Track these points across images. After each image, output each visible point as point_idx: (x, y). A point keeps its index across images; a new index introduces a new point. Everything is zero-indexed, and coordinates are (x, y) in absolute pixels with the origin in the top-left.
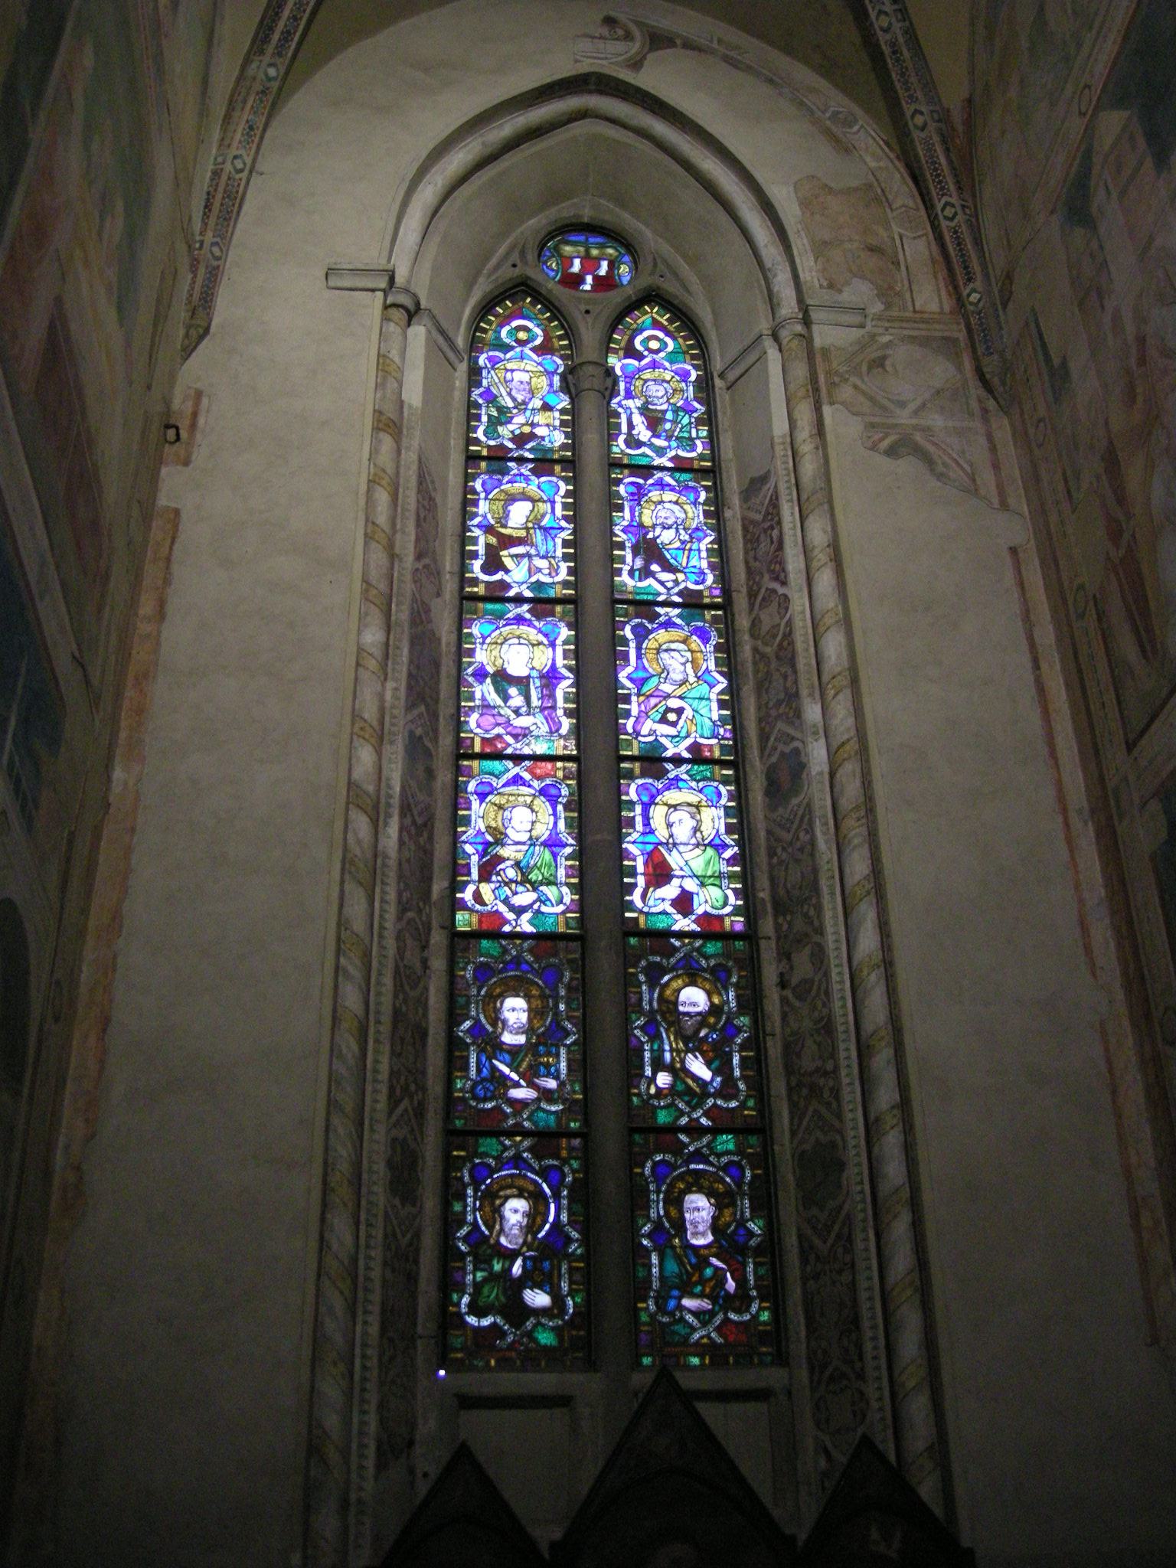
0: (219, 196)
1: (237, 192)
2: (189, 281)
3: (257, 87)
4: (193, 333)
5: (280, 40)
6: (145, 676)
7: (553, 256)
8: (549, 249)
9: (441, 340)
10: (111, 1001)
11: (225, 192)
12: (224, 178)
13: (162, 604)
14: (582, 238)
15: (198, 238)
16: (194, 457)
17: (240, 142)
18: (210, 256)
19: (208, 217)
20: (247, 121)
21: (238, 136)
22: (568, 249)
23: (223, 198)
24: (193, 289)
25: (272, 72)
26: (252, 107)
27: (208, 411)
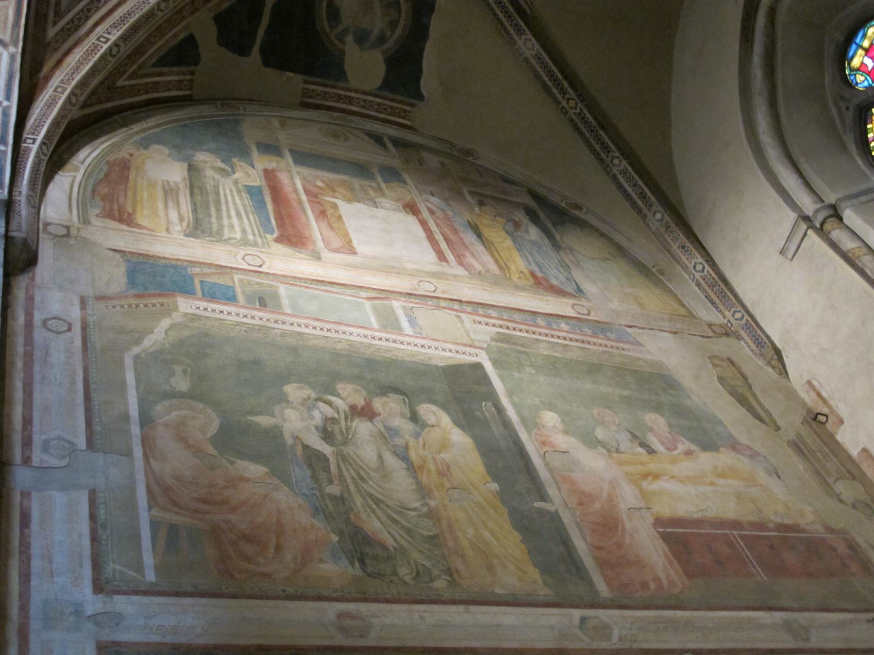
0: (709, 291)
1: (714, 279)
2: (745, 345)
3: (662, 230)
4: (775, 363)
5: (643, 202)
7: (855, 75)
8: (850, 75)
9: (863, 199)
11: (709, 286)
12: (702, 282)
14: (854, 47)
15: (726, 322)
16: (841, 415)
17: (687, 259)
18: (738, 322)
19: (718, 307)
20: (678, 247)
21: (684, 258)
22: (856, 63)
23: (712, 290)
24: (749, 346)
25: (658, 216)
26: (672, 240)
27: (821, 387)
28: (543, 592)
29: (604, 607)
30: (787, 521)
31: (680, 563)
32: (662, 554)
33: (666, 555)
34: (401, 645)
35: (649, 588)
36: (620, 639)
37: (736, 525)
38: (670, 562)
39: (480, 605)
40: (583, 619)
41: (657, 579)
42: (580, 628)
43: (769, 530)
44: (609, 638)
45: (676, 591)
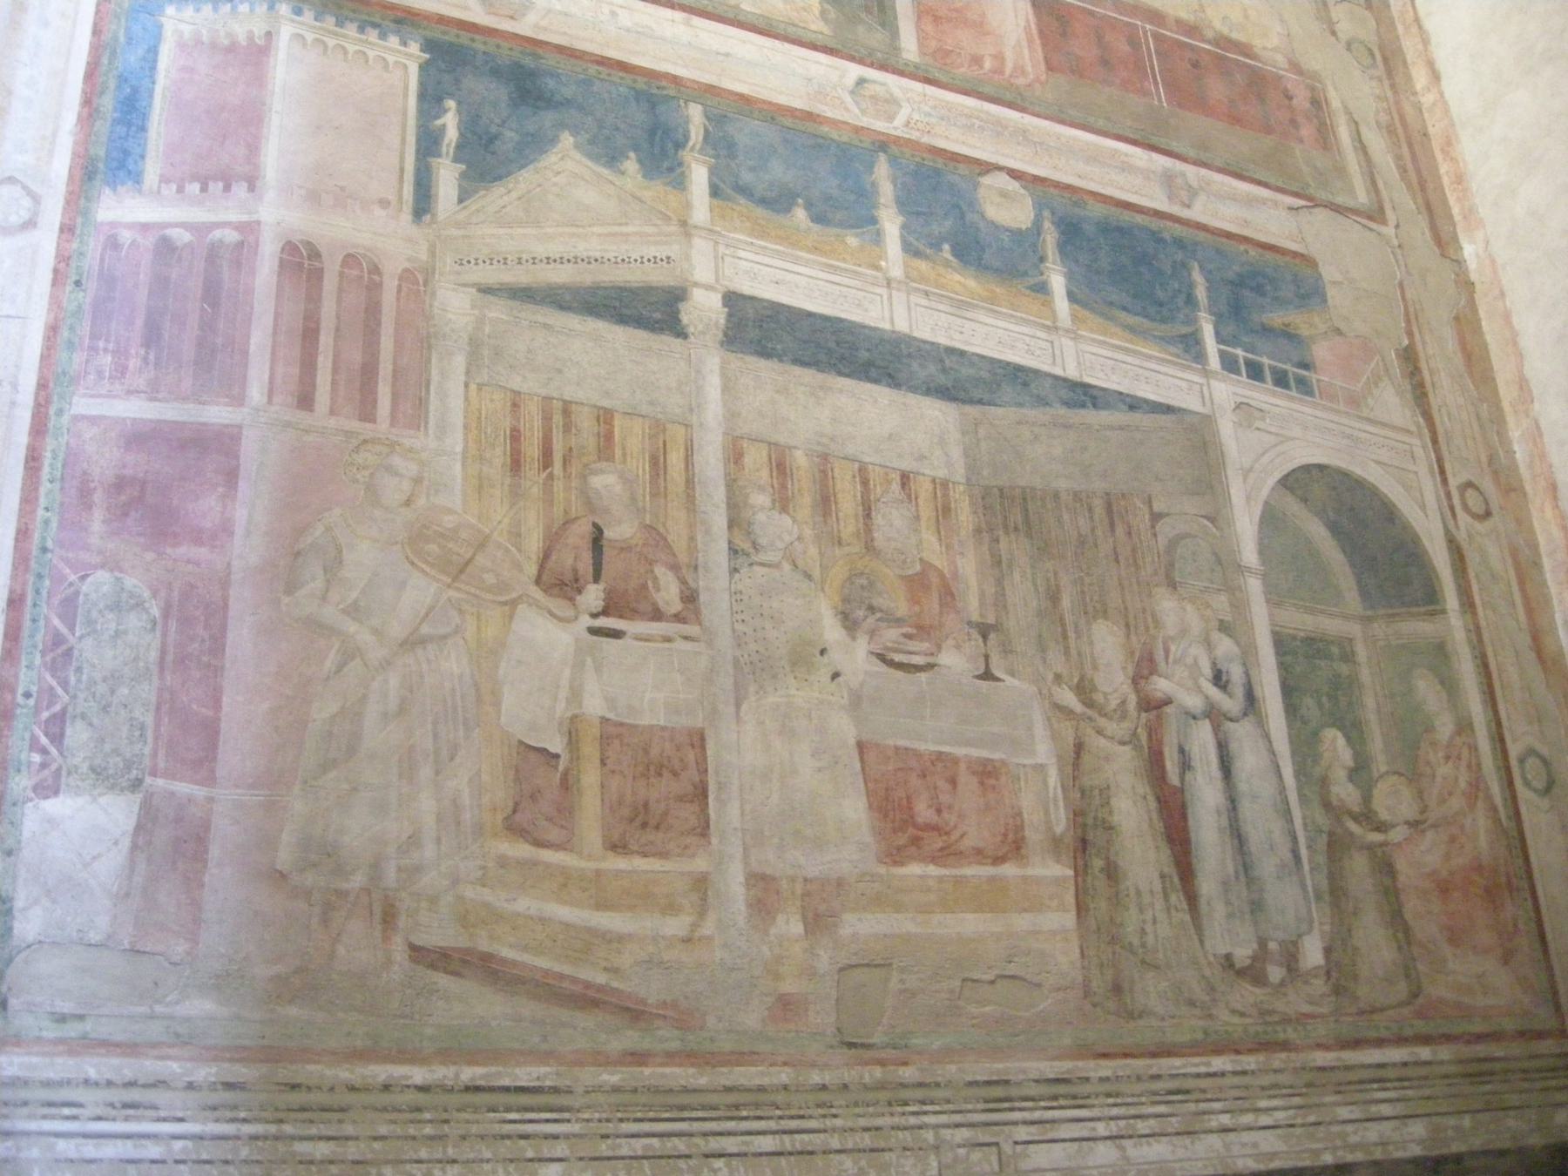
6: (1449, 142)
10: (1551, 466)
13: (1431, 65)
28: (818, 27)
29: (902, 73)
30: (1235, 35)
31: (1044, 45)
32: (1022, 24)
33: (1027, 29)
35: (981, 67)
36: (907, 124)
37: (1156, 17)
38: (1030, 41)
39: (719, 21)
40: (861, 82)
41: (999, 58)
42: (852, 92)
43: (1203, 41)
44: (891, 118)
45: (1021, 81)
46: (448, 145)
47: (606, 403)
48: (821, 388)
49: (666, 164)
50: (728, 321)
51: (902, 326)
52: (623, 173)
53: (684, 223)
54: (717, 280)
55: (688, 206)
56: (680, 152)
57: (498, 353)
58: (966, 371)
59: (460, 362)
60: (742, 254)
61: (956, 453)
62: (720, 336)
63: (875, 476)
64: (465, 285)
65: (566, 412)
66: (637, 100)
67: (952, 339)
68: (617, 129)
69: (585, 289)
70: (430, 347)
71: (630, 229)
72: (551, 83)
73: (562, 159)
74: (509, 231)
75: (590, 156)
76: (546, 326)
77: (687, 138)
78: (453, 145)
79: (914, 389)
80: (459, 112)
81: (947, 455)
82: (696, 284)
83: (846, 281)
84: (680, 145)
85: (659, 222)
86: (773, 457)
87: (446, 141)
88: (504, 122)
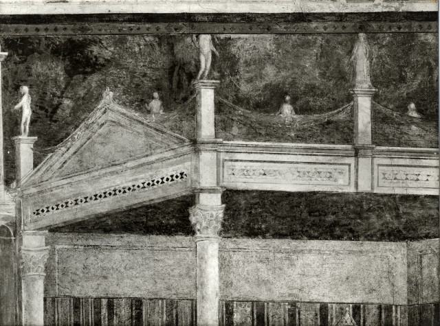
34: (107, 12)
46: (26, 122)
47: (137, 294)
48: (294, 252)
49: (182, 95)
50: (225, 214)
51: (364, 187)
52: (149, 112)
53: (194, 142)
54: (218, 183)
55: (197, 127)
56: (193, 82)
57: (64, 272)
58: (417, 213)
59: (40, 286)
60: (238, 156)
61: (401, 284)
62: (219, 227)
63: (333, 312)
64: (41, 229)
65: (110, 306)
66: (160, 45)
67: (408, 188)
68: (145, 75)
69: (121, 213)
70: (20, 279)
71: (153, 158)
72: (95, 49)
73: (105, 112)
74: (69, 180)
75: (124, 104)
76: (96, 247)
77: (198, 67)
78: (28, 122)
79: (370, 238)
80: (30, 93)
81: (393, 285)
82: (202, 190)
83: (321, 159)
84: (192, 76)
85: (176, 146)
86: (255, 311)
87: (23, 120)
88: (63, 93)
